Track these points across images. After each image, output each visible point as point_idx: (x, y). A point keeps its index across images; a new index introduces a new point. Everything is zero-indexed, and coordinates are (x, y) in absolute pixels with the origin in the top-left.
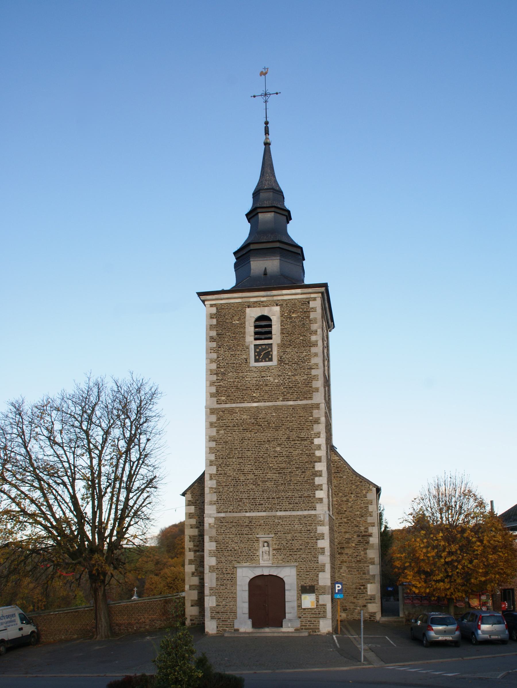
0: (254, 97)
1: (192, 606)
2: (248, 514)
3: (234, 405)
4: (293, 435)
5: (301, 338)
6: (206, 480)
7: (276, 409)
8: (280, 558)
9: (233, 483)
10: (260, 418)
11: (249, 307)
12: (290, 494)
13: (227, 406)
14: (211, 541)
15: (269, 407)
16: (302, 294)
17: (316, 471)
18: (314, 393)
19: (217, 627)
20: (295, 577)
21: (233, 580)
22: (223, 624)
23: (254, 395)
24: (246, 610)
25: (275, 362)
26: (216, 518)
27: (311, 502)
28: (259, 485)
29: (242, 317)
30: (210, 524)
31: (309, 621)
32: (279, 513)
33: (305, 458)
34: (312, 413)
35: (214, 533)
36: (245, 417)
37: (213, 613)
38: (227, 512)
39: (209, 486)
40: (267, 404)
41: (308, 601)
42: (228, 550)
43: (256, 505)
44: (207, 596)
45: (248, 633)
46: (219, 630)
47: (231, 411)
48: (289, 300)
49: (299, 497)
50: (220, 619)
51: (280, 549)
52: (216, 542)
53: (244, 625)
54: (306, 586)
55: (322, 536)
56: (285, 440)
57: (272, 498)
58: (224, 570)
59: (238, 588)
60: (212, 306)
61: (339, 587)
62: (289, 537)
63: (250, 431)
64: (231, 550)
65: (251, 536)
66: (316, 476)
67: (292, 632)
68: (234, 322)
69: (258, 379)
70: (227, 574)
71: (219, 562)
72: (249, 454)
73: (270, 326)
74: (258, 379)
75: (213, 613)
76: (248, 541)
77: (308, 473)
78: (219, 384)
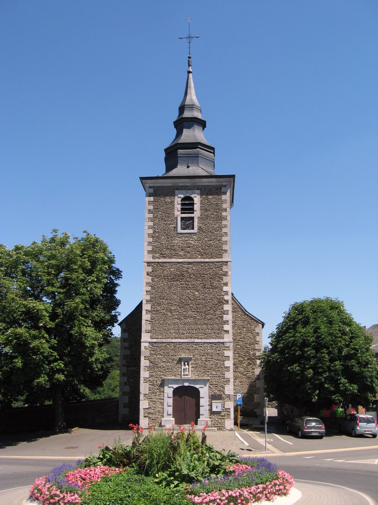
0: (181, 38)
1: (124, 407)
8: (196, 374)
11: (177, 190)
12: (205, 327)
25: (196, 230)
27: (221, 332)
32: (196, 340)
41: (217, 406)
43: (180, 334)
44: (142, 400)
51: (197, 367)
57: (192, 329)
61: (239, 396)
64: (160, 367)
71: (151, 376)
73: (193, 204)
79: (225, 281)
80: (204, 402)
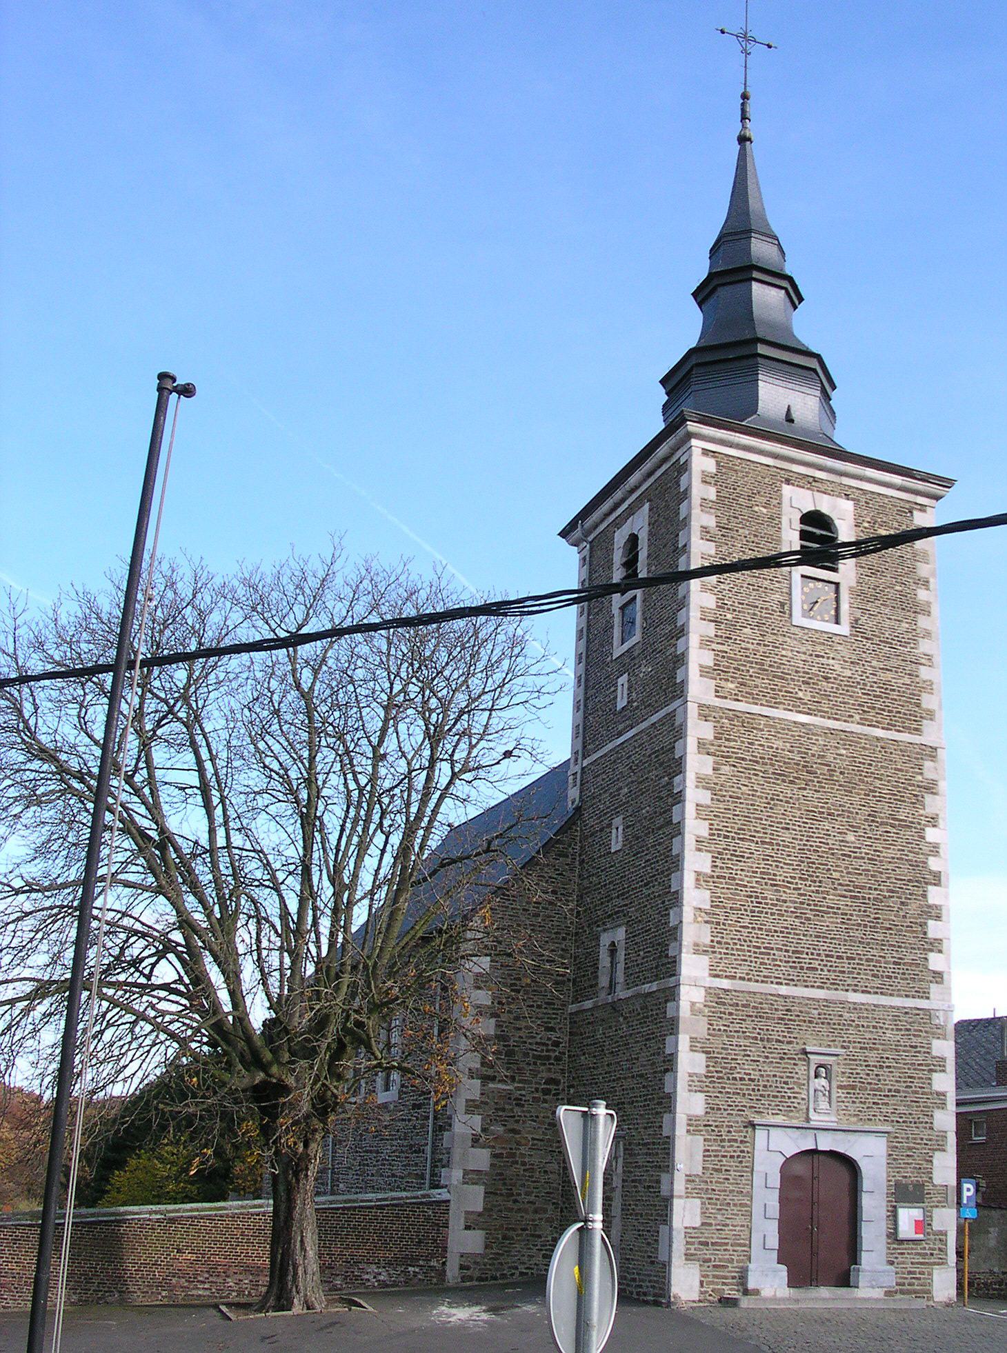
1: (467, 1228)
2: (783, 990)
3: (756, 709)
4: (885, 810)
5: (898, 588)
6: (685, 885)
7: (848, 739)
8: (851, 1107)
9: (750, 906)
10: (813, 755)
11: (788, 482)
12: (874, 952)
13: (741, 706)
14: (693, 1049)
15: (832, 731)
16: (900, 489)
17: (929, 906)
18: (925, 722)
19: (702, 1283)
20: (884, 1161)
21: (745, 1160)
22: (714, 1276)
23: (801, 694)
24: (774, 1242)
26: (708, 990)
28: (809, 919)
29: (775, 502)
30: (693, 1004)
31: (910, 1273)
33: (905, 871)
34: (920, 767)
35: (702, 1029)
36: (779, 744)
37: (693, 1243)
38: (734, 978)
39: (695, 904)
40: (831, 724)
42: (735, 1079)
43: (802, 968)
44: (680, 1197)
45: (782, 1300)
46: (706, 1292)
47: (747, 722)
48: (873, 493)
49: (895, 963)
50: (710, 1260)
51: (853, 1087)
52: (707, 1053)
53: (770, 1281)
54: (906, 1186)
55: (940, 1064)
56: (866, 820)
57: (838, 957)
58: (724, 1131)
59: (758, 1181)
60: (706, 452)
61: (968, 1190)
62: (873, 1057)
63: (791, 782)
64: (741, 1079)
65: (789, 1047)
66: (931, 917)
67: (877, 1300)
68: (756, 509)
69: (809, 659)
70: (729, 1141)
71: (711, 1109)
72: (787, 836)
74: (809, 659)
75: (693, 1243)
76: (782, 1058)
77: (913, 908)
78: (720, 647)
79: (929, 811)
80: (873, 1205)
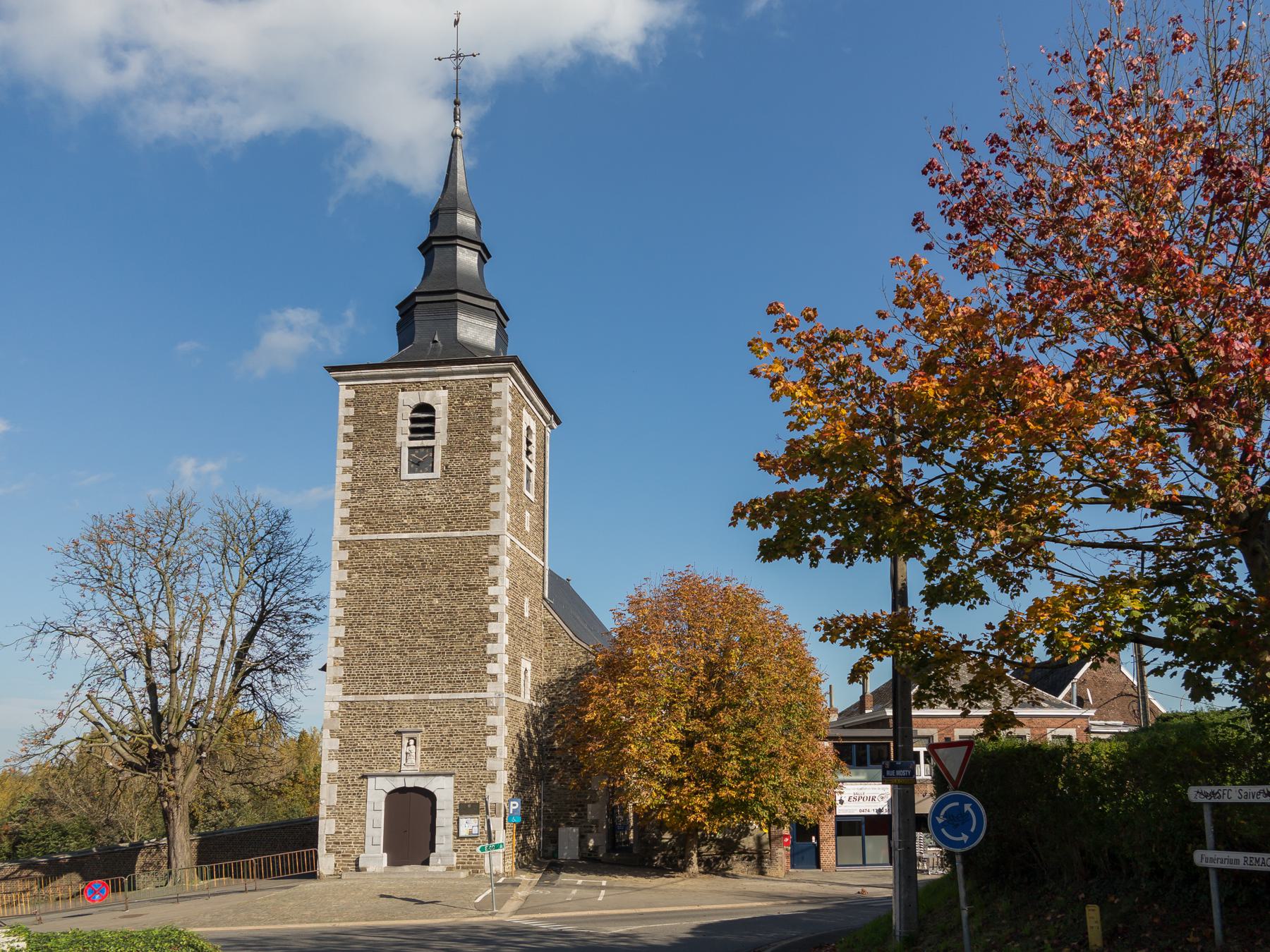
2: (388, 697)
3: (374, 537)
4: (459, 582)
11: (403, 390)
20: (452, 791)
21: (362, 796)
25: (437, 472)
27: (478, 677)
32: (433, 696)
34: (486, 550)
41: (469, 825)
60: (348, 387)
71: (342, 768)
72: (393, 608)
73: (432, 420)
77: (477, 638)
79: (491, 575)
80: (445, 817)
